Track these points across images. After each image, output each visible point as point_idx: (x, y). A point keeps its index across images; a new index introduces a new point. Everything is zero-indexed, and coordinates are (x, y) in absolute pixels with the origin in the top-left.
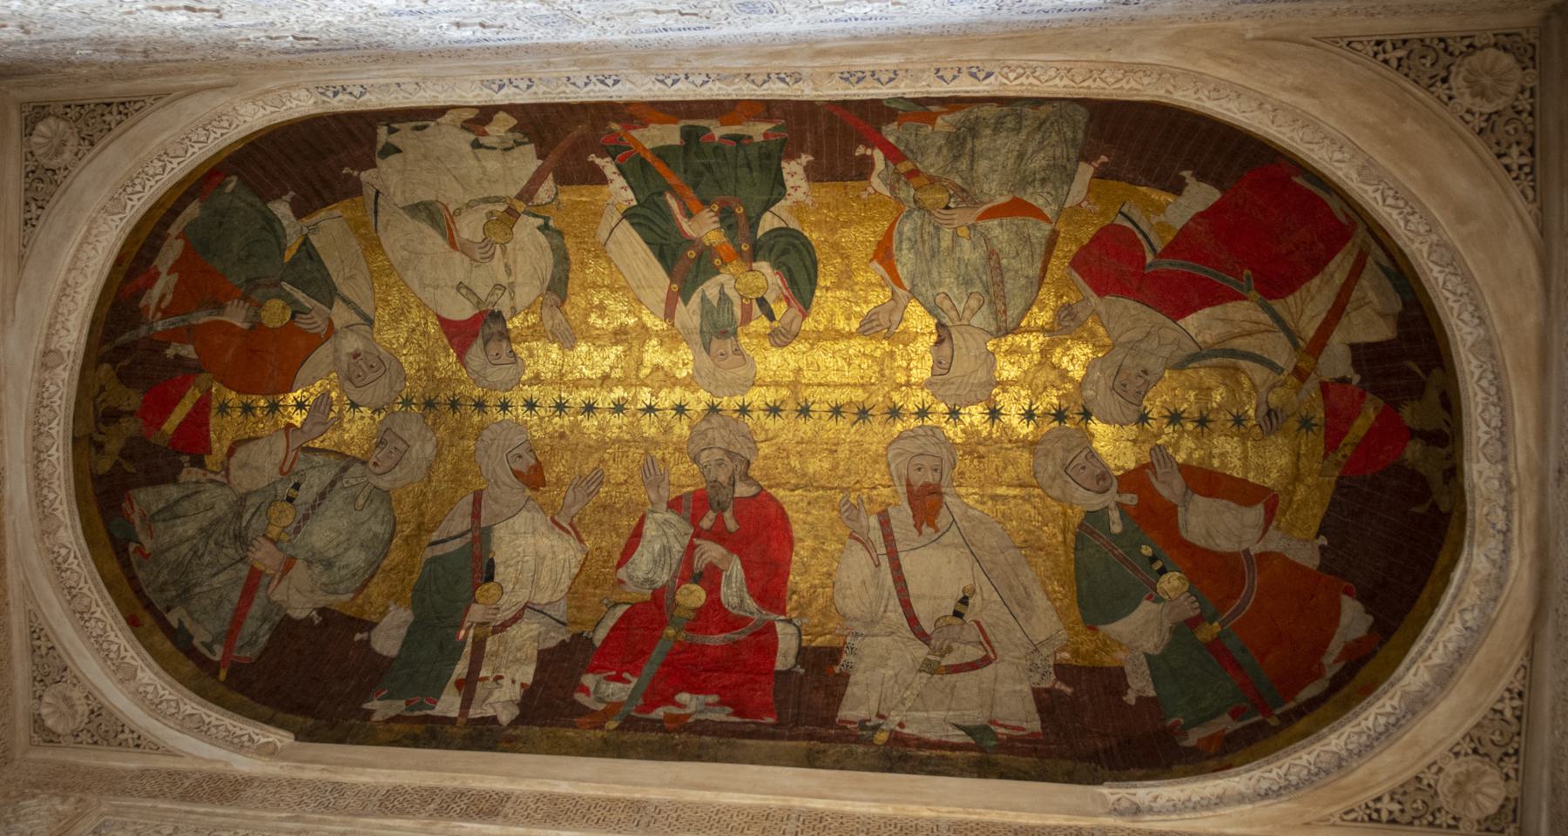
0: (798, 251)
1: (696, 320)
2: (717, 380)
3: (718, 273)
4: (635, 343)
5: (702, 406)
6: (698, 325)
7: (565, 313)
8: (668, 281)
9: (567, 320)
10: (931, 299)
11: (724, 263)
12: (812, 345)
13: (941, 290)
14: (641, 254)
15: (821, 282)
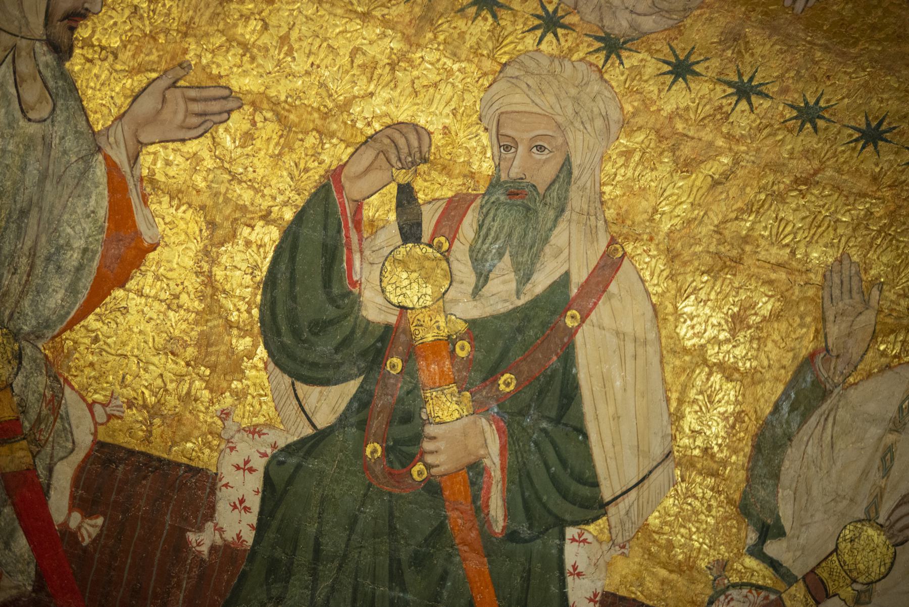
0: (292, 320)
1: (559, 237)
2: (576, 100)
3: (472, 324)
4: (705, 230)
5: (631, 60)
6: (562, 225)
7: (821, 333)
8: (579, 338)
9: (824, 320)
10: (60, 117)
11: (451, 341)
12: (345, 106)
13: (33, 128)
14: (606, 411)
15: (271, 235)
